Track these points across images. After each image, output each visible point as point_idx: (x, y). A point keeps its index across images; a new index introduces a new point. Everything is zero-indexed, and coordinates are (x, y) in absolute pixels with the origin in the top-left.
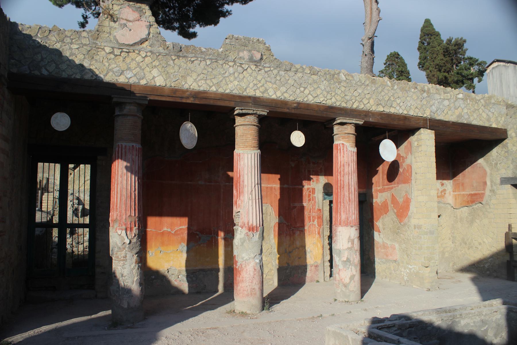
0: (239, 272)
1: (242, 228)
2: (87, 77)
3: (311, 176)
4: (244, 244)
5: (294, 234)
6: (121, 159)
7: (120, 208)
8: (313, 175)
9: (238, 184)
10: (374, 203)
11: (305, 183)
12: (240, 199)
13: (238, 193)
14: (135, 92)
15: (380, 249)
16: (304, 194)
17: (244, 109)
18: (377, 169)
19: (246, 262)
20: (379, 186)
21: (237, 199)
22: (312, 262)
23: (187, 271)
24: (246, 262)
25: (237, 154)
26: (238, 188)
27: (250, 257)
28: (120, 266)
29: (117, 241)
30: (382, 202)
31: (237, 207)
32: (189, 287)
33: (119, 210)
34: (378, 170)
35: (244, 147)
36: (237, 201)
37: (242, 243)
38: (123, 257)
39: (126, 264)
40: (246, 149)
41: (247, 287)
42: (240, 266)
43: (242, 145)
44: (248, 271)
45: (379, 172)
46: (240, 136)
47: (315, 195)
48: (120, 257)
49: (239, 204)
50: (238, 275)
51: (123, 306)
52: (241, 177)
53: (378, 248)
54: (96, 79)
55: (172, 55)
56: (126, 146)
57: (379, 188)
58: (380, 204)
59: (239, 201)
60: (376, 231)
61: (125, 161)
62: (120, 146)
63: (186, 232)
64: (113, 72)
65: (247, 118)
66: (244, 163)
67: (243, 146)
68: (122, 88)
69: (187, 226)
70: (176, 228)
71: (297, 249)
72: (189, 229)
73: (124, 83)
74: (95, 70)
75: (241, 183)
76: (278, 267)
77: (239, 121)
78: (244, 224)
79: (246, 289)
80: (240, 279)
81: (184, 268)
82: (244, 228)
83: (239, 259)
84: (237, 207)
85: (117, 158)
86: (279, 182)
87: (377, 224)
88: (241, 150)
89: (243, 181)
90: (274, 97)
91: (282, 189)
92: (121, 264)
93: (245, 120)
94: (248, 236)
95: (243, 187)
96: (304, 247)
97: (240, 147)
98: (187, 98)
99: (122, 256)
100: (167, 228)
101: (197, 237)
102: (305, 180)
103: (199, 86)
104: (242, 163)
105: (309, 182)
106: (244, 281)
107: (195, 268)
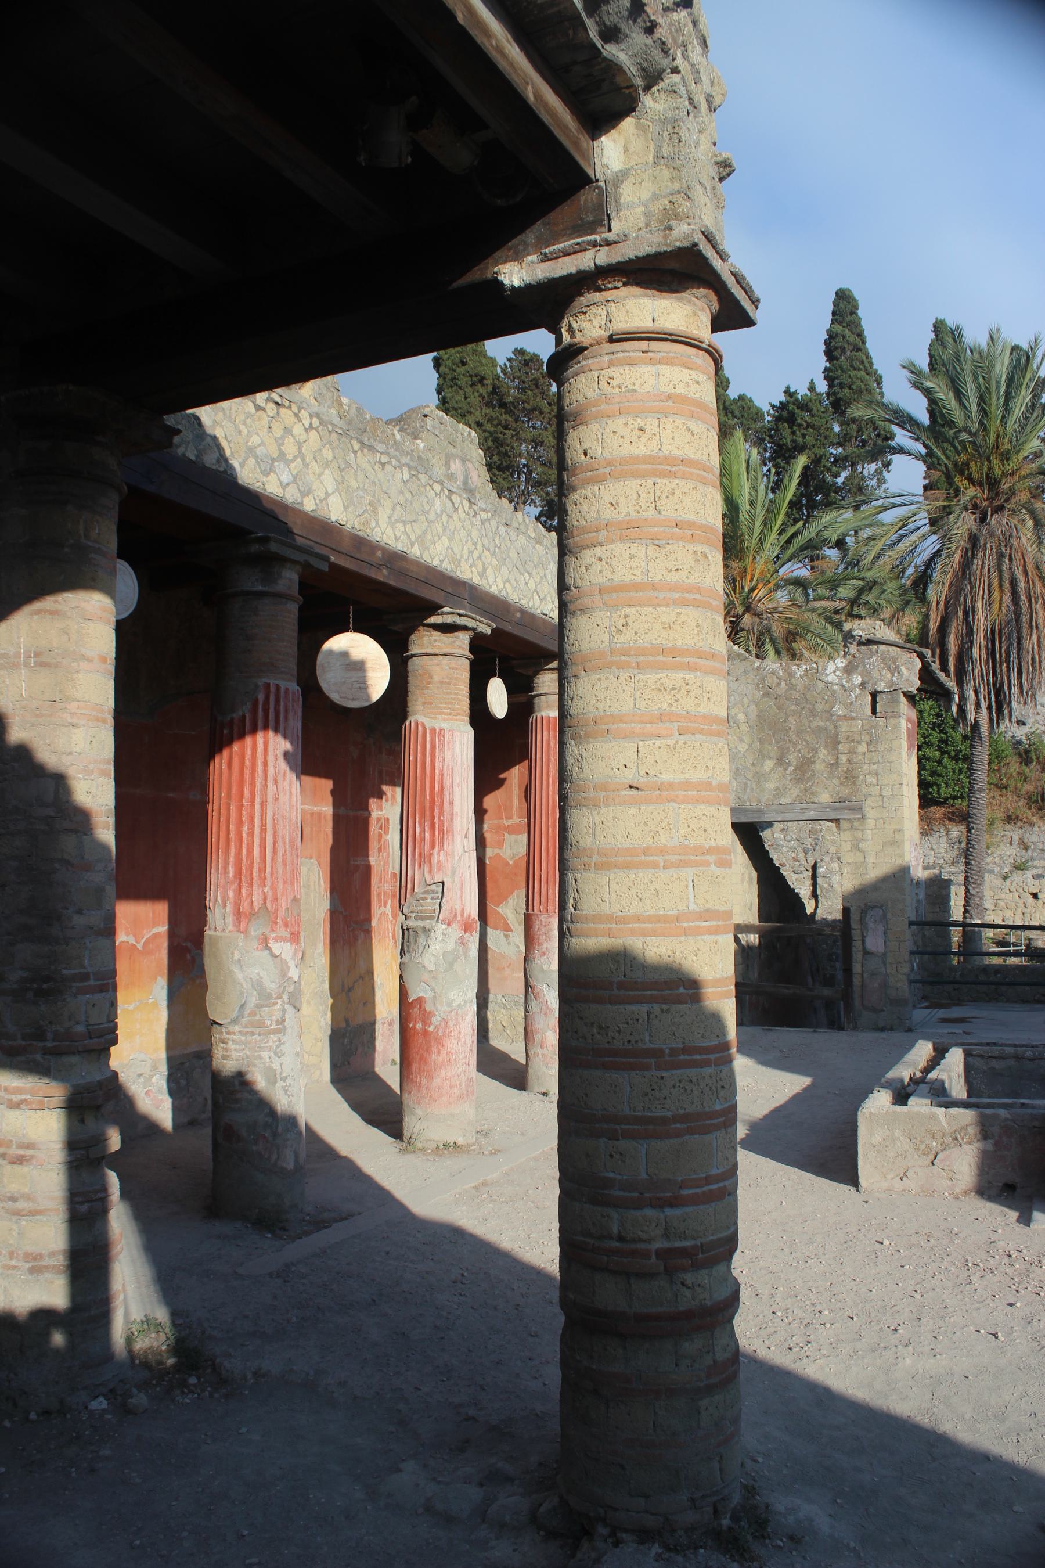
0: (440, 1042)
1: (449, 924)
2: (210, 460)
3: (384, 788)
4: (456, 966)
5: (356, 938)
6: (276, 731)
7: (272, 874)
8: (387, 784)
9: (436, 811)
10: (490, 858)
11: (373, 803)
12: (442, 848)
13: (437, 832)
14: (295, 531)
15: (507, 972)
16: (371, 833)
17: (466, 616)
18: (502, 776)
19: (457, 1014)
20: (511, 818)
21: (433, 847)
22: (385, 1015)
23: (170, 1060)
24: (457, 1014)
25: (433, 730)
26: (436, 821)
27: (466, 999)
28: (270, 1049)
29: (263, 974)
30: (517, 858)
31: (430, 872)
32: (176, 1109)
33: (268, 882)
34: (505, 779)
35: (450, 714)
36: (431, 855)
37: (451, 965)
38: (278, 1022)
39: (284, 1043)
40: (457, 720)
41: (458, 1076)
42: (443, 1025)
43: (445, 708)
44: (462, 1034)
45: (507, 783)
46: (442, 683)
47: (389, 837)
48: (268, 1023)
49: (439, 861)
50: (434, 1050)
51: (284, 1165)
52: (446, 793)
53: (500, 969)
54: (225, 472)
55: (352, 438)
56: (287, 689)
57: (506, 823)
58: (511, 862)
59: (439, 854)
60: (496, 929)
61: (285, 737)
62: (273, 689)
63: (165, 944)
64: (256, 457)
65: (457, 637)
66: (453, 756)
67: (449, 711)
68: (272, 511)
69: (167, 927)
70: (145, 931)
71: (361, 980)
72: (172, 934)
73: (272, 496)
74: (224, 443)
75: (446, 806)
76: (329, 1032)
77: (437, 644)
78: (455, 915)
79: (458, 1083)
80: (440, 1059)
81: (163, 1055)
82: (455, 925)
83: (437, 1005)
84: (430, 872)
85: (260, 723)
86: (330, 799)
87: (499, 909)
88: (444, 720)
89: (451, 803)
90: (494, 590)
91: (337, 818)
92: (270, 1044)
93: (454, 642)
94: (463, 944)
95: (452, 819)
96: (370, 973)
97: (441, 714)
98: (378, 567)
99: (274, 1018)
100: (127, 934)
101: (188, 957)
102: (374, 797)
103: (397, 539)
104: (448, 755)
105: (379, 801)
106: (453, 1062)
107: (186, 1052)
